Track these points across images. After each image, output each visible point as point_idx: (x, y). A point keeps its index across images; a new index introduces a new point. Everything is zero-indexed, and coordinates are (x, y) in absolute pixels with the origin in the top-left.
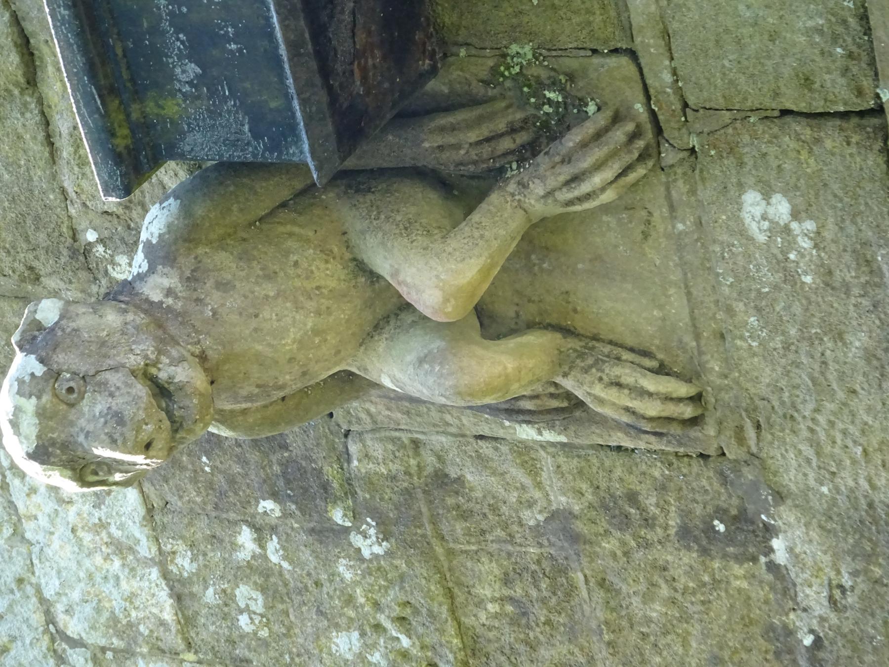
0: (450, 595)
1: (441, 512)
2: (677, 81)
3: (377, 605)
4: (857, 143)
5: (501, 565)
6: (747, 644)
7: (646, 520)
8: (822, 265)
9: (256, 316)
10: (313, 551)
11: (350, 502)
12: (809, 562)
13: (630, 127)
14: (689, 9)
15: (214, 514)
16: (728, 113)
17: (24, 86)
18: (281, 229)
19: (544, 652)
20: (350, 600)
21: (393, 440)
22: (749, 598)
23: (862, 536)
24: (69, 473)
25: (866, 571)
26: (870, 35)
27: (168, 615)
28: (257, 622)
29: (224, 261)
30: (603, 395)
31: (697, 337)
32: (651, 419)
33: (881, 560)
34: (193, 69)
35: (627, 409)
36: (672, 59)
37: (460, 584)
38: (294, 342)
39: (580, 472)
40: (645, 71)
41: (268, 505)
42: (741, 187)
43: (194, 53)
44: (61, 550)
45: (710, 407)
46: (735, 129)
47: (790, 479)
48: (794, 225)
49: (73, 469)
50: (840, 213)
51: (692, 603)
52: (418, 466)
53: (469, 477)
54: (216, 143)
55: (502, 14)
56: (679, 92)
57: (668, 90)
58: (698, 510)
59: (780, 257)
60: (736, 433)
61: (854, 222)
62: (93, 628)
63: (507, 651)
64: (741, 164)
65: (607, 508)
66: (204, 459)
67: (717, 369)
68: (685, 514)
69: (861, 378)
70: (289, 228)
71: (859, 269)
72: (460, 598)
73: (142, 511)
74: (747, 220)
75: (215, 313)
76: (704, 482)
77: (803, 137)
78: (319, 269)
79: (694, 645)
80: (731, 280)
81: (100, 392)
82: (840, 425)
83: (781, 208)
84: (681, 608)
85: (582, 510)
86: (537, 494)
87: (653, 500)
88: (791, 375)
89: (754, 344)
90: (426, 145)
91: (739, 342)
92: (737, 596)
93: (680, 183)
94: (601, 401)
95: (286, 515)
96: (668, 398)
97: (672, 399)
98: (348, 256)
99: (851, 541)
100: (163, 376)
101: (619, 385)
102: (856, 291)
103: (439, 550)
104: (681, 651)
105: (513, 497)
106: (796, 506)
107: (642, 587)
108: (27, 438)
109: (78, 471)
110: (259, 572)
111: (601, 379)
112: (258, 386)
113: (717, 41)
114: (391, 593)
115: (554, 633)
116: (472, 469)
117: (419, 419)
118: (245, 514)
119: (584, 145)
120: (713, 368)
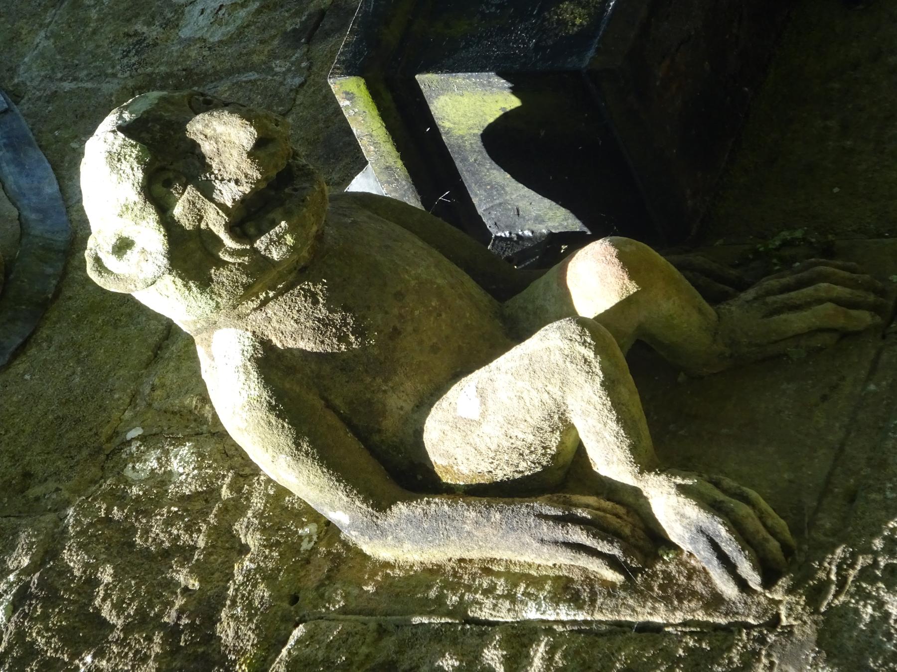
52: (367, 656)
67: (828, 525)
101: (717, 484)
120: (823, 525)
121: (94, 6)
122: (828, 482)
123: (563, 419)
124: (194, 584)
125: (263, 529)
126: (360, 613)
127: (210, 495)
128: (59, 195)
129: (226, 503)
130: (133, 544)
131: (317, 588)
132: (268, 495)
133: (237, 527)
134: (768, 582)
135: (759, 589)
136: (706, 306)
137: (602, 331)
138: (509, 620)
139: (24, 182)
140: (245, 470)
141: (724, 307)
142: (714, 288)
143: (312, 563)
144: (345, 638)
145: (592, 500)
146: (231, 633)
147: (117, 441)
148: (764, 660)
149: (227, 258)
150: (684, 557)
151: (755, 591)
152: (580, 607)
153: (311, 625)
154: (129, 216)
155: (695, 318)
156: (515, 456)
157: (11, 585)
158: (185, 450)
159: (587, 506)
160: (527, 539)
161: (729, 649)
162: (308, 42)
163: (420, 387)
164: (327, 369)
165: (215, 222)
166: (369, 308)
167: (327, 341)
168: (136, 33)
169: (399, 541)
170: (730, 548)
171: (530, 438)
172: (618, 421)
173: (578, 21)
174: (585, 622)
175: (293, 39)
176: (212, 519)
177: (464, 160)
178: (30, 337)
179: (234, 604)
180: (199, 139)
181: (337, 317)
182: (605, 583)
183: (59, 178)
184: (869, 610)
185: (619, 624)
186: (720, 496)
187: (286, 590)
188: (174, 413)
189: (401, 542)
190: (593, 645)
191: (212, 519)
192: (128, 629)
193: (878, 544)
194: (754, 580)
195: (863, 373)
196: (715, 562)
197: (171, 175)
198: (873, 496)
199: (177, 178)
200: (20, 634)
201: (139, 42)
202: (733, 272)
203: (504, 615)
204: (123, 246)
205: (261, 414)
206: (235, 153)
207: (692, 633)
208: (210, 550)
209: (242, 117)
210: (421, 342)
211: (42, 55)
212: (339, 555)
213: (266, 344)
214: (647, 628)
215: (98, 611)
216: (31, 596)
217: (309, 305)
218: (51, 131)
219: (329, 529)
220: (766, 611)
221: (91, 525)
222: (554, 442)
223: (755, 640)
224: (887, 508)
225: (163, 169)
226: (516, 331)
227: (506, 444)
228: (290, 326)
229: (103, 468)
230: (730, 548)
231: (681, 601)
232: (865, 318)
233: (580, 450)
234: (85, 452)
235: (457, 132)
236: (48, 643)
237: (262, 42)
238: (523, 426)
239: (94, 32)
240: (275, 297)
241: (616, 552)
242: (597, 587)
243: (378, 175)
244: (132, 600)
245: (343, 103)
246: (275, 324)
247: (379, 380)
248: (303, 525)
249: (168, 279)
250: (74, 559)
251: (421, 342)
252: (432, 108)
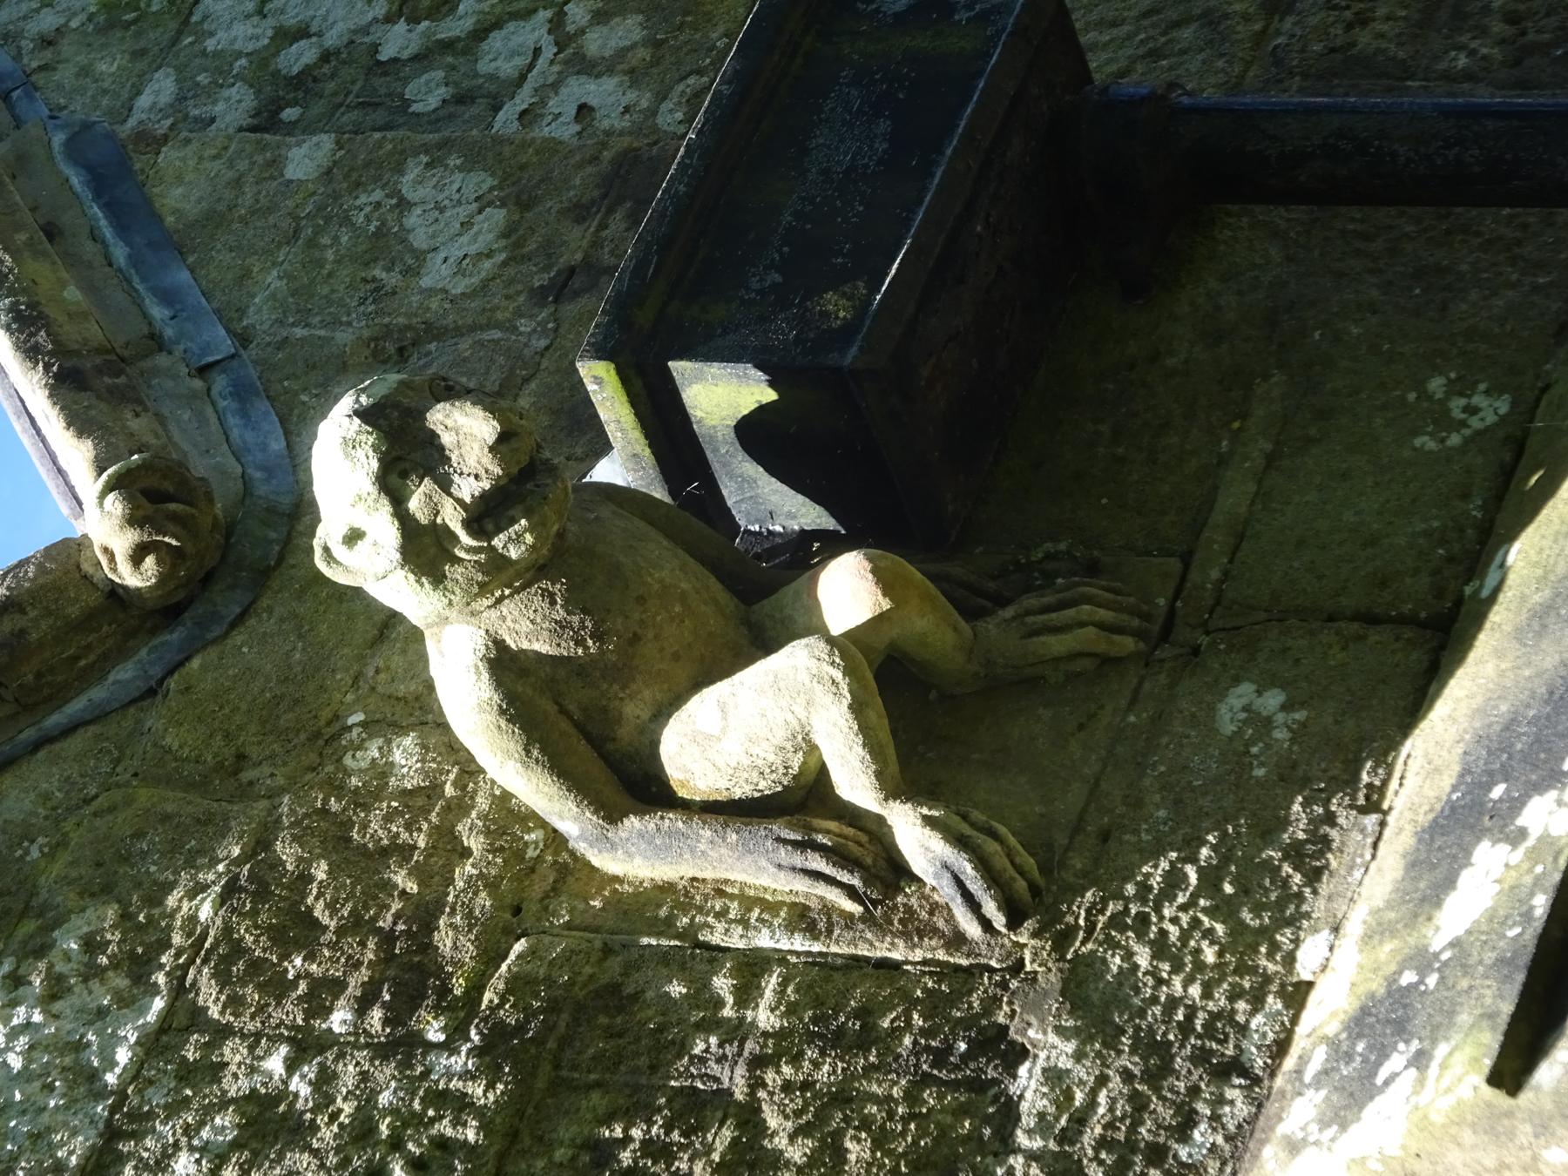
36: (1231, 561)
52: (591, 976)
72: (527, 1141)
89: (1144, 837)
101: (965, 817)
109: (394, 454)
121: (331, 246)
122: (1081, 819)
123: (807, 740)
124: (412, 887)
125: (487, 833)
126: (585, 930)
127: (432, 791)
128: (285, 452)
129: (449, 801)
130: (350, 839)
131: (542, 899)
132: (494, 796)
133: (459, 827)
134: (1014, 923)
135: (1004, 930)
136: (962, 623)
137: (854, 649)
138: (741, 945)
139: (249, 436)
140: (470, 770)
141: (980, 624)
142: (971, 603)
143: (537, 875)
144: (569, 956)
145: (833, 825)
146: (449, 943)
147: (337, 726)
148: (1005, 1007)
149: (462, 555)
150: (927, 890)
151: (999, 933)
152: (816, 938)
153: (533, 939)
154: (361, 506)
155: (950, 637)
156: (755, 774)
157: (220, 875)
158: (409, 741)
159: (827, 832)
160: (763, 863)
161: (970, 993)
162: (556, 301)
163: (658, 696)
164: (562, 673)
165: (452, 517)
166: (609, 611)
167: (563, 644)
168: (374, 279)
169: (630, 855)
170: (976, 886)
171: (771, 758)
172: (864, 745)
173: (842, 314)
174: (820, 954)
175: (540, 296)
176: (434, 817)
177: (716, 450)
178: (249, 606)
179: (453, 912)
180: (439, 430)
181: (575, 619)
182: (842, 913)
183: (287, 433)
184: (1118, 960)
185: (856, 959)
186: (967, 830)
187: (508, 901)
188: (398, 699)
189: (633, 856)
190: (827, 980)
191: (434, 817)
192: (341, 932)
193: (1130, 889)
194: (999, 921)
195: (1124, 703)
196: (959, 900)
197: (407, 465)
198: (1127, 837)
199: (414, 470)
200: (227, 930)
201: (377, 289)
202: (992, 586)
203: (736, 941)
204: (353, 537)
205: (491, 717)
206: (476, 446)
207: (931, 973)
208: (430, 851)
209: (485, 409)
210: (662, 650)
211: (273, 296)
212: (565, 865)
213: (499, 644)
214: (884, 964)
215: (310, 910)
216: (242, 889)
217: (546, 605)
218: (281, 381)
219: (556, 839)
220: (1009, 954)
221: (306, 815)
222: (796, 762)
223: (997, 985)
224: (1140, 851)
225: (399, 459)
226: (762, 641)
227: (746, 762)
228: (525, 626)
229: (321, 754)
230: (976, 886)
231: (921, 938)
232: (1128, 644)
233: (823, 771)
234: (303, 736)
235: (710, 422)
236: (256, 941)
237: (507, 297)
238: (765, 745)
239: (330, 275)
240: (511, 595)
241: (856, 882)
242: (835, 918)
243: (622, 466)
244: (346, 900)
245: (591, 387)
246: (509, 622)
247: (616, 687)
248: (529, 830)
249: (403, 573)
250: (287, 852)
251: (662, 650)
252: (684, 396)
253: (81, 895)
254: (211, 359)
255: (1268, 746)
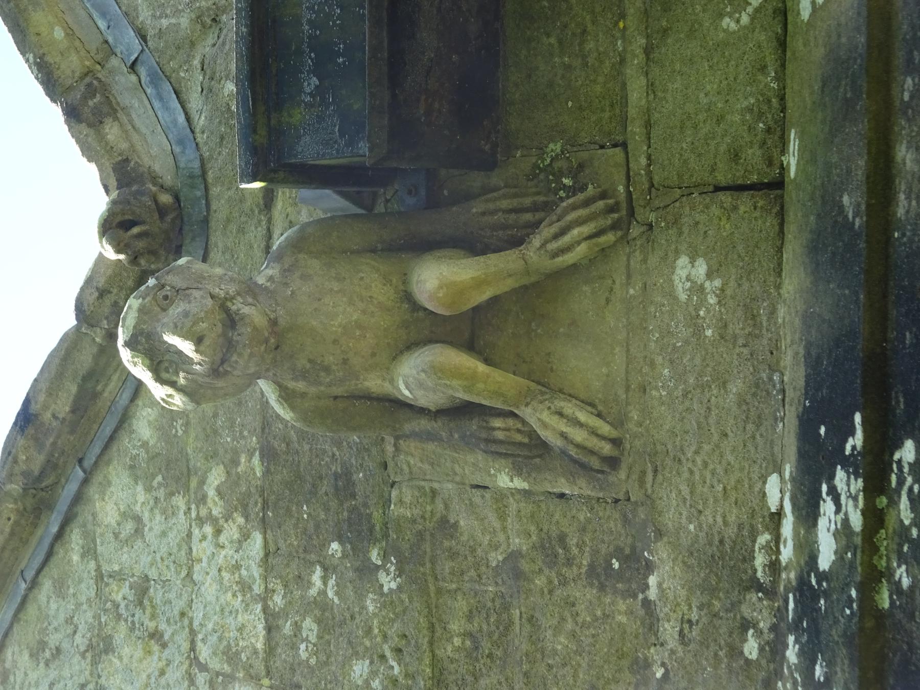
0: (432, 628)
1: (438, 552)
2: (649, 165)
3: (385, 637)
4: (762, 207)
5: (468, 603)
6: (617, 675)
7: (568, 559)
8: (722, 318)
9: (320, 300)
10: (354, 587)
11: (384, 543)
12: (671, 596)
13: (611, 201)
14: (667, 102)
15: (302, 556)
16: (678, 191)
17: (262, 207)
18: (364, 260)
19: (483, 682)
20: (369, 631)
21: (420, 488)
22: (625, 632)
23: (711, 571)
24: (147, 362)
25: (710, 605)
26: (784, 113)
27: (260, 646)
28: (310, 649)
29: (314, 265)
30: (547, 420)
31: (628, 388)
32: (578, 446)
33: (721, 594)
34: (315, 81)
35: (563, 435)
36: (649, 147)
37: (440, 620)
38: (340, 326)
39: (532, 516)
40: (630, 155)
41: (335, 546)
42: (677, 253)
43: (316, 70)
44: (210, 589)
45: (626, 453)
46: (681, 202)
47: (669, 519)
48: (707, 284)
49: (151, 360)
50: (740, 271)
51: (586, 636)
52: (431, 512)
53: (462, 523)
54: (317, 144)
55: (548, 117)
56: (649, 173)
57: (643, 172)
58: (603, 551)
59: (694, 313)
60: (640, 478)
61: (748, 280)
62: (214, 653)
63: (460, 683)
64: (680, 234)
65: (543, 547)
66: (305, 508)
67: (636, 417)
68: (595, 552)
69: (732, 421)
70: (368, 261)
71: (746, 321)
72: (439, 632)
73: (262, 554)
74: (676, 278)
75: (293, 292)
76: (612, 524)
77: (725, 205)
78: (376, 286)
79: (581, 676)
80: (657, 335)
81: (183, 301)
82: (711, 467)
83: (701, 268)
84: (579, 641)
85: (528, 550)
86: (501, 537)
87: (575, 541)
88: (685, 421)
89: (664, 393)
90: (474, 210)
91: (654, 393)
92: (617, 629)
93: (637, 253)
94: (545, 426)
95: (345, 556)
96: (594, 433)
97: (597, 435)
98: (402, 288)
99: (702, 575)
100: (234, 308)
101: (561, 414)
102: (741, 341)
103: (432, 588)
104: (571, 682)
105: (486, 540)
106: (669, 543)
107: (555, 622)
108: (127, 329)
109: (155, 363)
110: (321, 605)
111: (549, 408)
112: (310, 361)
113: (681, 128)
114: (396, 625)
115: (492, 665)
116: (464, 515)
117: (438, 469)
118: (321, 555)
119: (574, 208)
253: (206, 459)
254: (133, 58)
255: (708, 311)
